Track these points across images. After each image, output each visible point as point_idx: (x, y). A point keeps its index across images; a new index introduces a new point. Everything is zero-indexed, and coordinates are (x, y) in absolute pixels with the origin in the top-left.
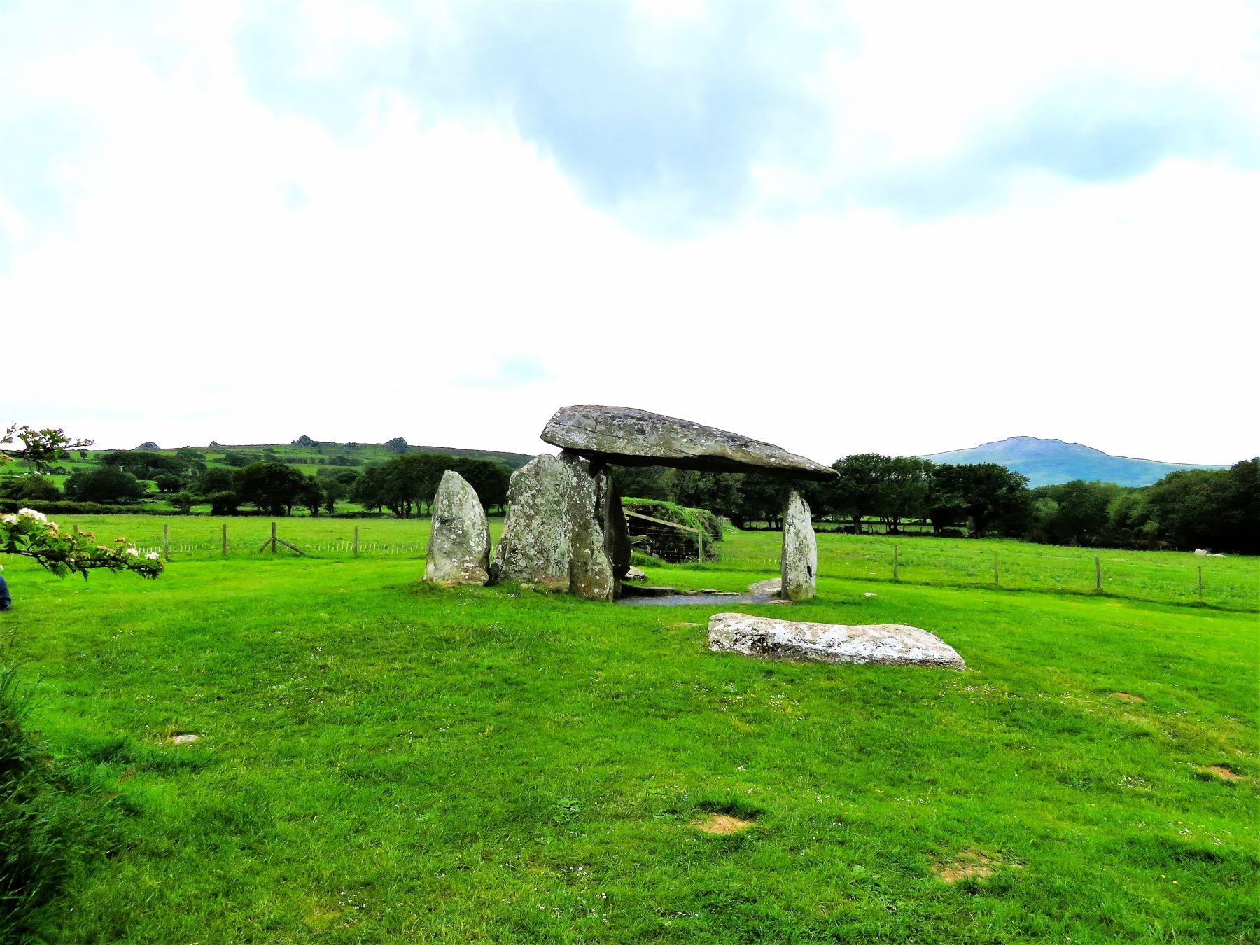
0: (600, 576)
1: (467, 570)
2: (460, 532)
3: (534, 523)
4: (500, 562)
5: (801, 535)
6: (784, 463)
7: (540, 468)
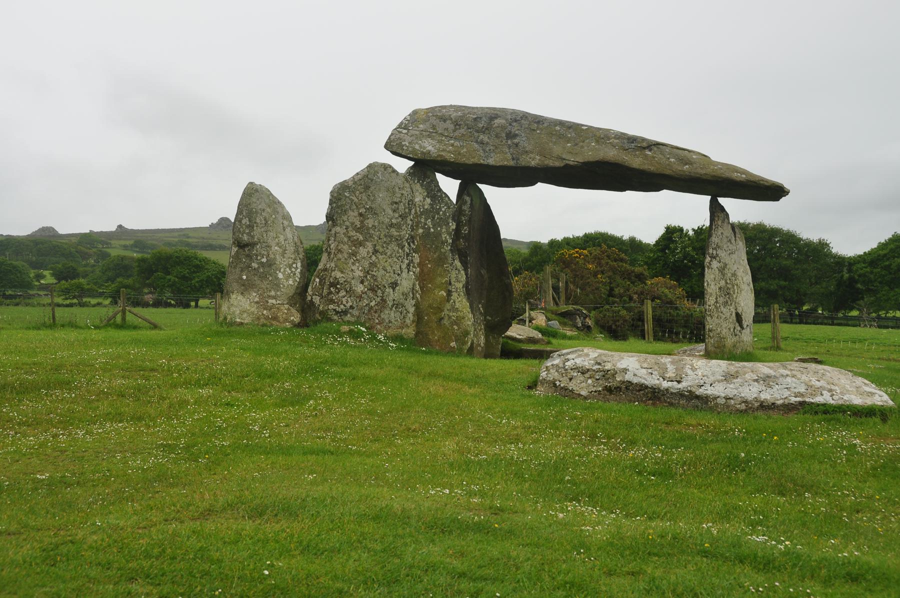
1: (270, 309)
3: (363, 252)
4: (317, 300)
6: (703, 172)
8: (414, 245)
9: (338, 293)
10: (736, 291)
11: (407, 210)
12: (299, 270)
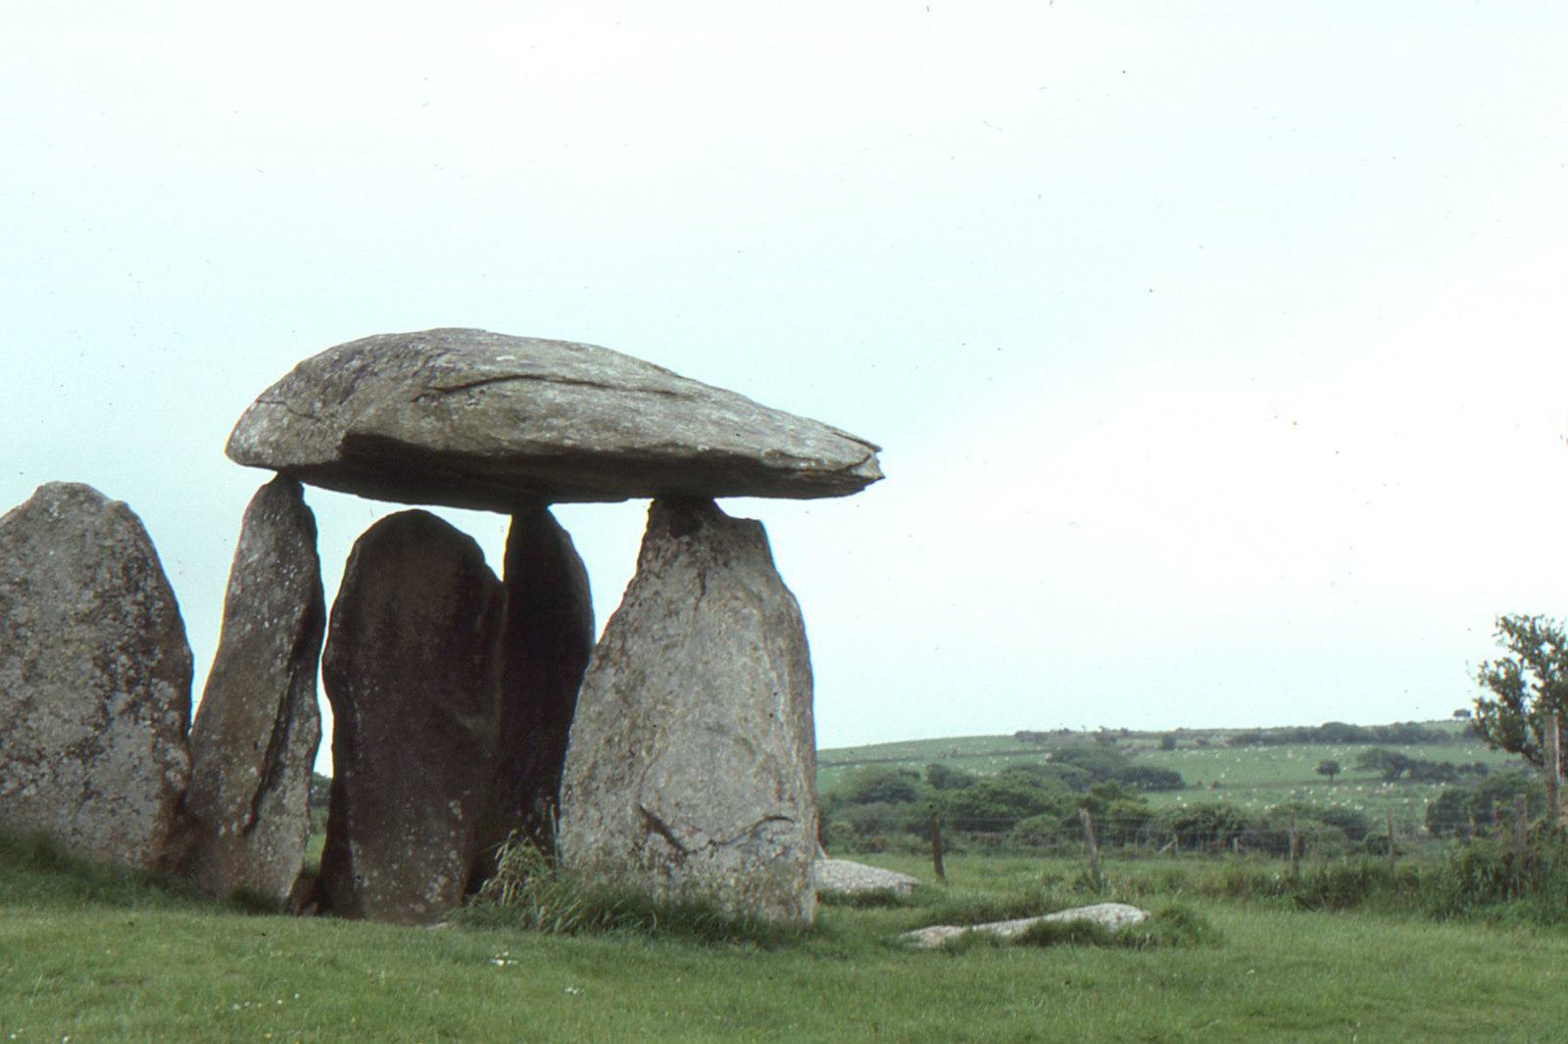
5: (645, 698)
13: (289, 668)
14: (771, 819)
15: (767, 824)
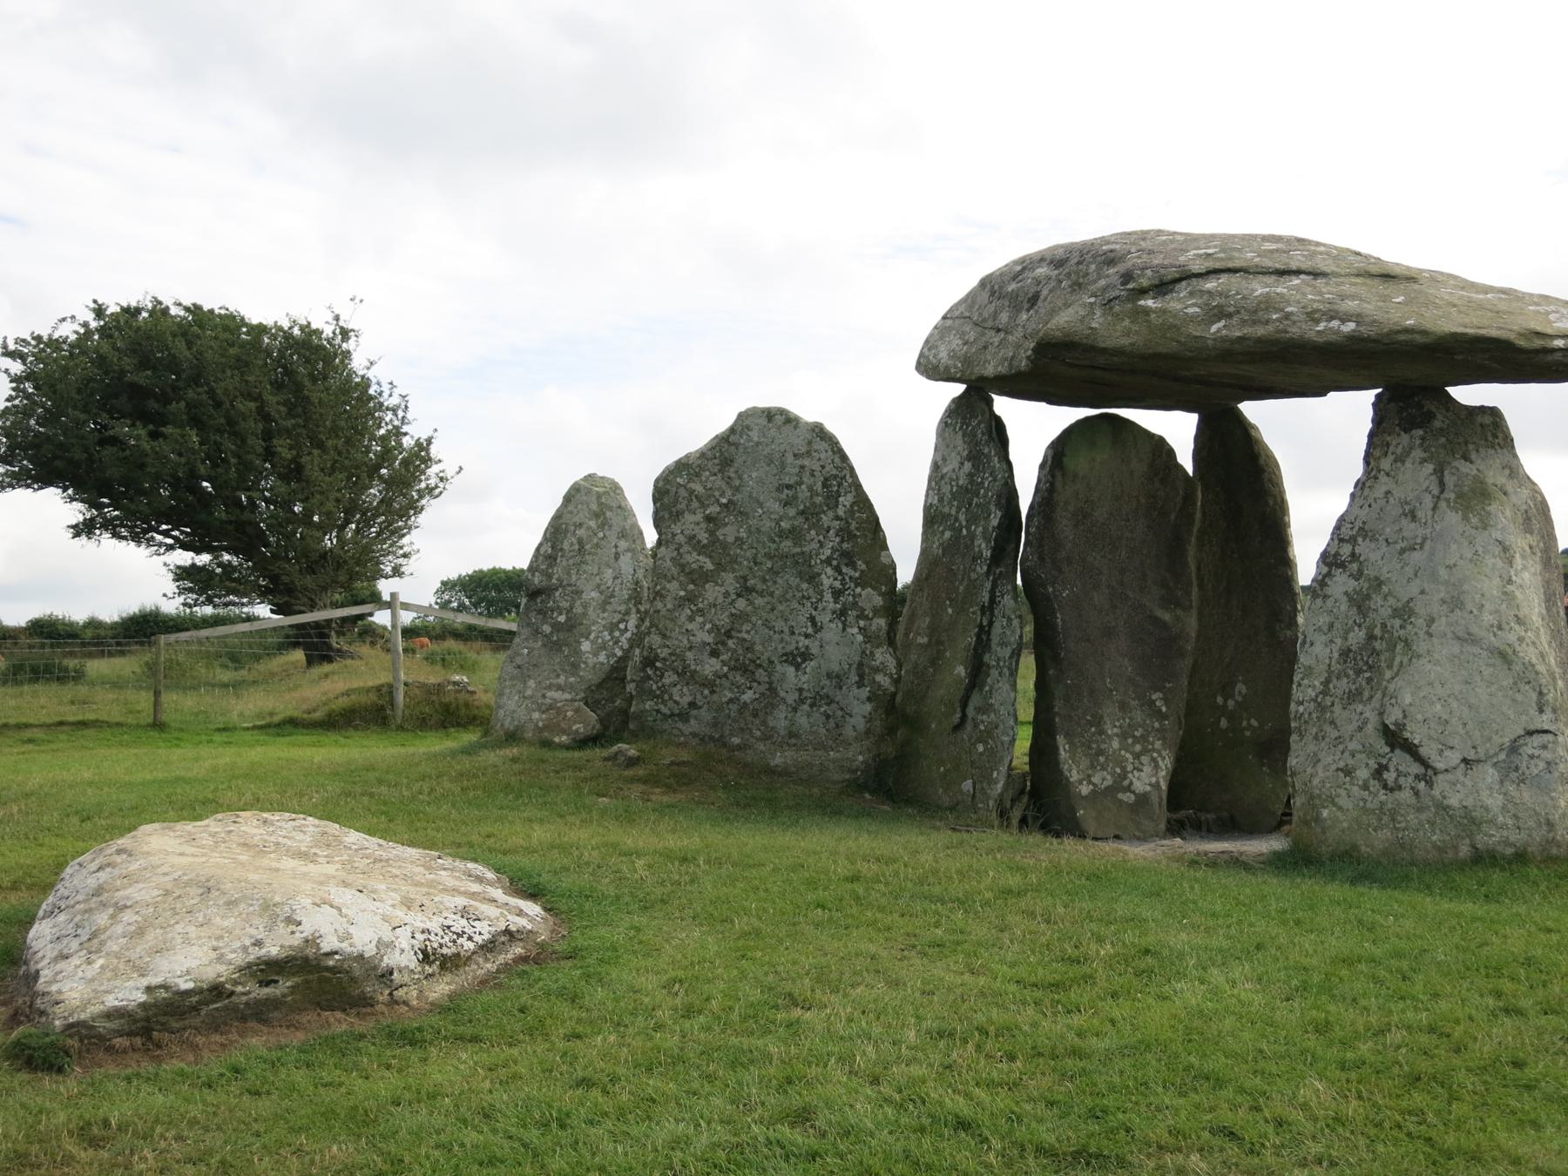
0: (985, 743)
2: (562, 619)
3: (712, 592)
5: (1382, 608)
7: (737, 445)
8: (855, 571)
9: (662, 676)
10: (1398, 660)
11: (819, 500)
12: (628, 635)
13: (988, 573)
14: (1530, 733)
15: (1528, 739)
